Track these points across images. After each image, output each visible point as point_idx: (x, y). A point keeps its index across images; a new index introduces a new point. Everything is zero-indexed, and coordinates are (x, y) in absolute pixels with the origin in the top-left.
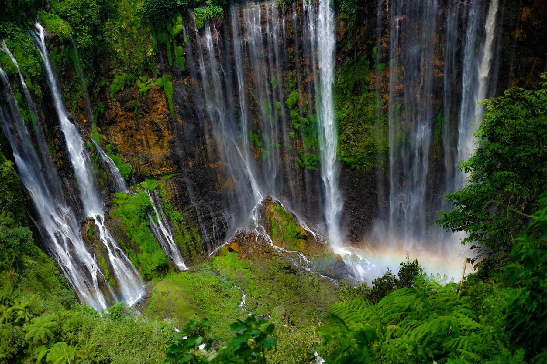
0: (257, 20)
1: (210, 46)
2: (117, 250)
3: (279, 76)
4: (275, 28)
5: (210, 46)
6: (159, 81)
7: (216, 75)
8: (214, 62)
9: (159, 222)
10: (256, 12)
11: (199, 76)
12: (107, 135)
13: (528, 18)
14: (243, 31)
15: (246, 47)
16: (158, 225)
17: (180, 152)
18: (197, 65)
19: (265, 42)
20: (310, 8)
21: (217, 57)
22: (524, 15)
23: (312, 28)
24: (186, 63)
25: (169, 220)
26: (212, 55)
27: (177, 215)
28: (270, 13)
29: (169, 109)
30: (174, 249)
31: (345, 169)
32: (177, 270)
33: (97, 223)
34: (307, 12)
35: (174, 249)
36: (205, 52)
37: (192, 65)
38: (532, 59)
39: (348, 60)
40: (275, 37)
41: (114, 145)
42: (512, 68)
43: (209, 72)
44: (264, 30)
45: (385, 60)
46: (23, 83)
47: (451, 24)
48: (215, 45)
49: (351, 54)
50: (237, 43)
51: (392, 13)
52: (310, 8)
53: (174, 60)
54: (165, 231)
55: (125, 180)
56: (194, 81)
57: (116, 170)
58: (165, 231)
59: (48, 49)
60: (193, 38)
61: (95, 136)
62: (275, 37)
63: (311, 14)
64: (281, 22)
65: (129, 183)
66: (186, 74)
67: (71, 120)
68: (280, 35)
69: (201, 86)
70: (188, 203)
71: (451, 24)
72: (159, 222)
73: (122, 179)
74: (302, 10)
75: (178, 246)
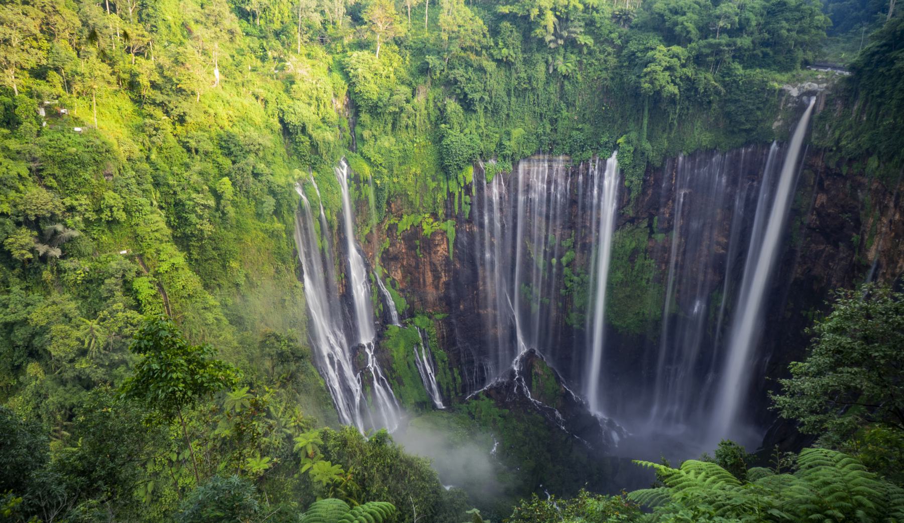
0: (543, 179)
1: (496, 198)
2: (382, 379)
3: (558, 233)
4: (559, 188)
5: (496, 198)
6: (443, 226)
7: (498, 225)
8: (497, 215)
9: (424, 358)
10: (543, 172)
11: (481, 225)
12: (388, 270)
13: (822, 205)
14: (528, 188)
15: (529, 202)
16: (423, 362)
17: (453, 294)
18: (481, 215)
20: (596, 173)
21: (501, 210)
22: (818, 202)
23: (595, 192)
24: (471, 213)
25: (433, 357)
26: (496, 207)
28: (557, 174)
29: (448, 252)
30: (434, 387)
31: (610, 331)
32: (434, 407)
33: (367, 350)
34: (593, 176)
35: (434, 387)
37: (476, 213)
38: (822, 247)
39: (628, 227)
40: (559, 196)
41: (394, 279)
42: (799, 254)
43: (491, 220)
44: (549, 189)
45: (669, 229)
46: (322, 213)
47: (738, 203)
48: (501, 198)
49: (632, 221)
50: (521, 198)
52: (596, 173)
53: (460, 207)
54: (428, 367)
55: (399, 314)
57: (391, 303)
58: (428, 367)
59: (349, 186)
60: (480, 189)
63: (596, 181)
64: (566, 183)
65: (401, 317)
66: (470, 221)
67: (359, 251)
68: (564, 196)
69: (482, 233)
70: (454, 344)
71: (738, 203)
72: (424, 358)
73: (395, 312)
74: (587, 174)
75: (439, 385)
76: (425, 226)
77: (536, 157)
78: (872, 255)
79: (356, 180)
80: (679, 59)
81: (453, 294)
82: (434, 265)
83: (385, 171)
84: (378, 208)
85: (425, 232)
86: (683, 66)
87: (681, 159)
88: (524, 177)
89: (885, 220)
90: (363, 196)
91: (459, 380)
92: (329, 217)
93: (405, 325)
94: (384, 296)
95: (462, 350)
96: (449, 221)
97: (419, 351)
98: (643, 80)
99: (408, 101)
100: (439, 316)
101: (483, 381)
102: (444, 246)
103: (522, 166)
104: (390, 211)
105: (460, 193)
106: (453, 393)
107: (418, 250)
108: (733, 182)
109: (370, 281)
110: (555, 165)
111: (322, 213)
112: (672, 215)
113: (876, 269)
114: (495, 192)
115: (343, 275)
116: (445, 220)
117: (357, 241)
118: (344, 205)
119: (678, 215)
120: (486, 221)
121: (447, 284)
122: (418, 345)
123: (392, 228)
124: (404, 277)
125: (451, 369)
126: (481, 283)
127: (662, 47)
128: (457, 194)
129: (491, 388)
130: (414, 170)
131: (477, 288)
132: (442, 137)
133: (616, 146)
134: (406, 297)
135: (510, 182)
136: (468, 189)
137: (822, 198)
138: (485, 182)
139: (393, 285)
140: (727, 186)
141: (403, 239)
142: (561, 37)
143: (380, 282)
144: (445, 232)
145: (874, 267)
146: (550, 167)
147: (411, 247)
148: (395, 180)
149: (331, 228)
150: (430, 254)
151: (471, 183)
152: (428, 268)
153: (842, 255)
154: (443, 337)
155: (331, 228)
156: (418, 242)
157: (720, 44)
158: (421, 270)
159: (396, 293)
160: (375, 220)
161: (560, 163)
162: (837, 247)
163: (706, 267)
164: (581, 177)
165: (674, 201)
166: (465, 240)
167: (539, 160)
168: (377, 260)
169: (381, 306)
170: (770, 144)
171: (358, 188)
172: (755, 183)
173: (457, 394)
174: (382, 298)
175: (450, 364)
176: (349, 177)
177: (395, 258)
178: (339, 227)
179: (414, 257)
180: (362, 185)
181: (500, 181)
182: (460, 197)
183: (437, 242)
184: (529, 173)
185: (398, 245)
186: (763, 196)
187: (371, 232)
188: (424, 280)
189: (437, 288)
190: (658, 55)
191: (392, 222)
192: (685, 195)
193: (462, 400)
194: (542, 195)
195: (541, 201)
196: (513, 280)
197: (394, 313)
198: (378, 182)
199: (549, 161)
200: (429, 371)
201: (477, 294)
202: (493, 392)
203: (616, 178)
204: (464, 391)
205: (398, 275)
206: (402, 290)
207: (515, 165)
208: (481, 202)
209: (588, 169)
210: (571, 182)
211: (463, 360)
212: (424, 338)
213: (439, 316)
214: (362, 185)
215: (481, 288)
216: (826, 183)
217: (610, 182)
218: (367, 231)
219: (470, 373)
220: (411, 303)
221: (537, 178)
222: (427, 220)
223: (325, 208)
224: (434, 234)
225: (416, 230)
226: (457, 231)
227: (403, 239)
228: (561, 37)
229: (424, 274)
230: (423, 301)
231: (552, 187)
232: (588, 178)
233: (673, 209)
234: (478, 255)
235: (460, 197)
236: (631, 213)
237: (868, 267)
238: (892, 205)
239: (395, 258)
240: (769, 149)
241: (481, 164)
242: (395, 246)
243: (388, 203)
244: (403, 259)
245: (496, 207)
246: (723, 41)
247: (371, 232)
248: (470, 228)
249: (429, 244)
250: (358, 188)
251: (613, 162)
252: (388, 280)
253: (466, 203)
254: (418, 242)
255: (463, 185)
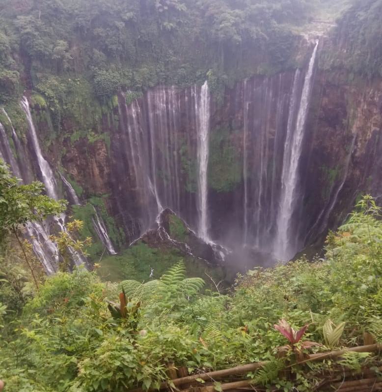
0: (163, 100)
3: (176, 135)
4: (174, 106)
6: (102, 137)
7: (137, 131)
8: (136, 126)
11: (127, 134)
12: (67, 168)
14: (154, 107)
15: (156, 116)
16: (99, 226)
18: (126, 128)
19: (168, 114)
20: (195, 95)
21: (138, 123)
22: (324, 102)
23: (196, 107)
24: (119, 126)
26: (135, 122)
27: (111, 219)
28: (172, 97)
30: (108, 241)
31: (212, 194)
33: (59, 224)
34: (193, 97)
35: (108, 241)
36: (131, 117)
37: (123, 127)
38: (327, 129)
39: (218, 127)
40: (174, 111)
43: (133, 130)
44: (167, 107)
45: (241, 128)
46: (14, 132)
48: (137, 115)
49: (219, 123)
50: (151, 115)
51: (245, 99)
53: (112, 122)
54: (102, 229)
55: (78, 197)
56: (124, 136)
57: (72, 191)
58: (102, 229)
59: (32, 113)
60: (124, 110)
61: (61, 170)
62: (174, 111)
64: (178, 103)
65: (80, 199)
67: (45, 158)
68: (176, 111)
71: (279, 106)
72: (99, 223)
73: (76, 196)
74: (190, 96)
75: (111, 239)
76: (89, 137)
77: (158, 87)
78: (354, 130)
79: (35, 108)
80: (241, 18)
81: (114, 180)
82: (99, 163)
83: (56, 101)
84: (55, 128)
85: (90, 141)
86: (243, 22)
87: (245, 82)
88: (151, 101)
89: (359, 110)
90: (42, 120)
91: (124, 234)
92: (20, 136)
93: (84, 203)
94: (67, 187)
95: (123, 215)
96: (105, 133)
97: (95, 220)
98: (219, 32)
99: (67, 51)
100: (106, 196)
101: (139, 233)
102: (104, 149)
103: (149, 95)
104: (64, 129)
105: (111, 114)
106: (120, 243)
107: (87, 154)
108: (276, 95)
109: (56, 177)
110: (169, 91)
111: (14, 132)
112: (242, 118)
113: (356, 138)
114: (133, 112)
115: (36, 175)
116: (102, 133)
117: (43, 152)
118: (30, 127)
119: (245, 118)
120: (130, 130)
121: (109, 174)
122: (93, 216)
123: (66, 141)
124: (79, 173)
125: (118, 228)
126: (131, 171)
127: (229, 11)
128: (108, 115)
129: (145, 236)
130: (77, 99)
131: (129, 175)
132: (94, 77)
133: (206, 78)
134: (82, 186)
135: (143, 104)
136: (115, 110)
137: (325, 100)
138: (126, 105)
139: (72, 178)
140: (272, 98)
141: (75, 147)
142: (166, 5)
143: (63, 178)
144: (104, 140)
145: (355, 136)
146: (167, 93)
147: (82, 153)
148: (65, 107)
149: (22, 143)
150: (95, 156)
151: (117, 107)
152: (95, 165)
153: (338, 132)
154: (110, 209)
155: (22, 143)
156: (85, 148)
157: (263, 8)
158: (90, 167)
159: (74, 183)
160: (54, 136)
161: (172, 91)
162: (335, 128)
163: (265, 148)
164: (186, 98)
165: (243, 109)
166: (117, 144)
167: (159, 89)
168: (59, 163)
169: (65, 193)
170: (295, 70)
171: (38, 114)
172: (288, 95)
173: (123, 244)
174: (66, 188)
175: (117, 225)
176: (30, 106)
177: (71, 160)
178: (28, 143)
179: (84, 159)
180: (41, 111)
181: (136, 104)
182: (111, 117)
183: (99, 148)
184: (154, 98)
185: (72, 152)
186: (293, 100)
187: (52, 144)
188: (93, 173)
189: (102, 177)
190: (228, 16)
191: (66, 136)
192: (249, 104)
193: (127, 247)
194: (163, 111)
195: (163, 116)
196: (151, 168)
197: (75, 197)
198: (53, 109)
199: (166, 89)
200: (103, 232)
201: (129, 179)
202: (146, 239)
203: (208, 97)
204: (128, 242)
205: (75, 172)
206: (78, 181)
207: (145, 93)
208: (126, 119)
209: (190, 93)
210: (181, 102)
211: (124, 222)
212: (97, 211)
213: (106, 196)
214: (41, 111)
215: (131, 174)
216: (327, 91)
217: (204, 99)
218: (49, 144)
219: (130, 229)
220: (86, 189)
221: (160, 100)
222: (90, 133)
223: (16, 130)
224: (96, 142)
225: (83, 143)
226: (111, 139)
227: (75, 147)
228: (166, 5)
229: (92, 169)
230: (94, 187)
231: (170, 106)
232: (191, 99)
233: (243, 113)
234: (127, 153)
235: (111, 117)
236: (219, 119)
237: (352, 137)
238: (362, 100)
239: (71, 160)
240: (295, 74)
241: (123, 94)
242: (71, 152)
243: (62, 124)
244: (77, 160)
245: (135, 122)
246: (265, 6)
247: (52, 144)
248: (120, 136)
249: (93, 149)
250: (38, 114)
251: (205, 87)
252: (68, 176)
253: (115, 120)
254: (85, 148)
255: (112, 108)
